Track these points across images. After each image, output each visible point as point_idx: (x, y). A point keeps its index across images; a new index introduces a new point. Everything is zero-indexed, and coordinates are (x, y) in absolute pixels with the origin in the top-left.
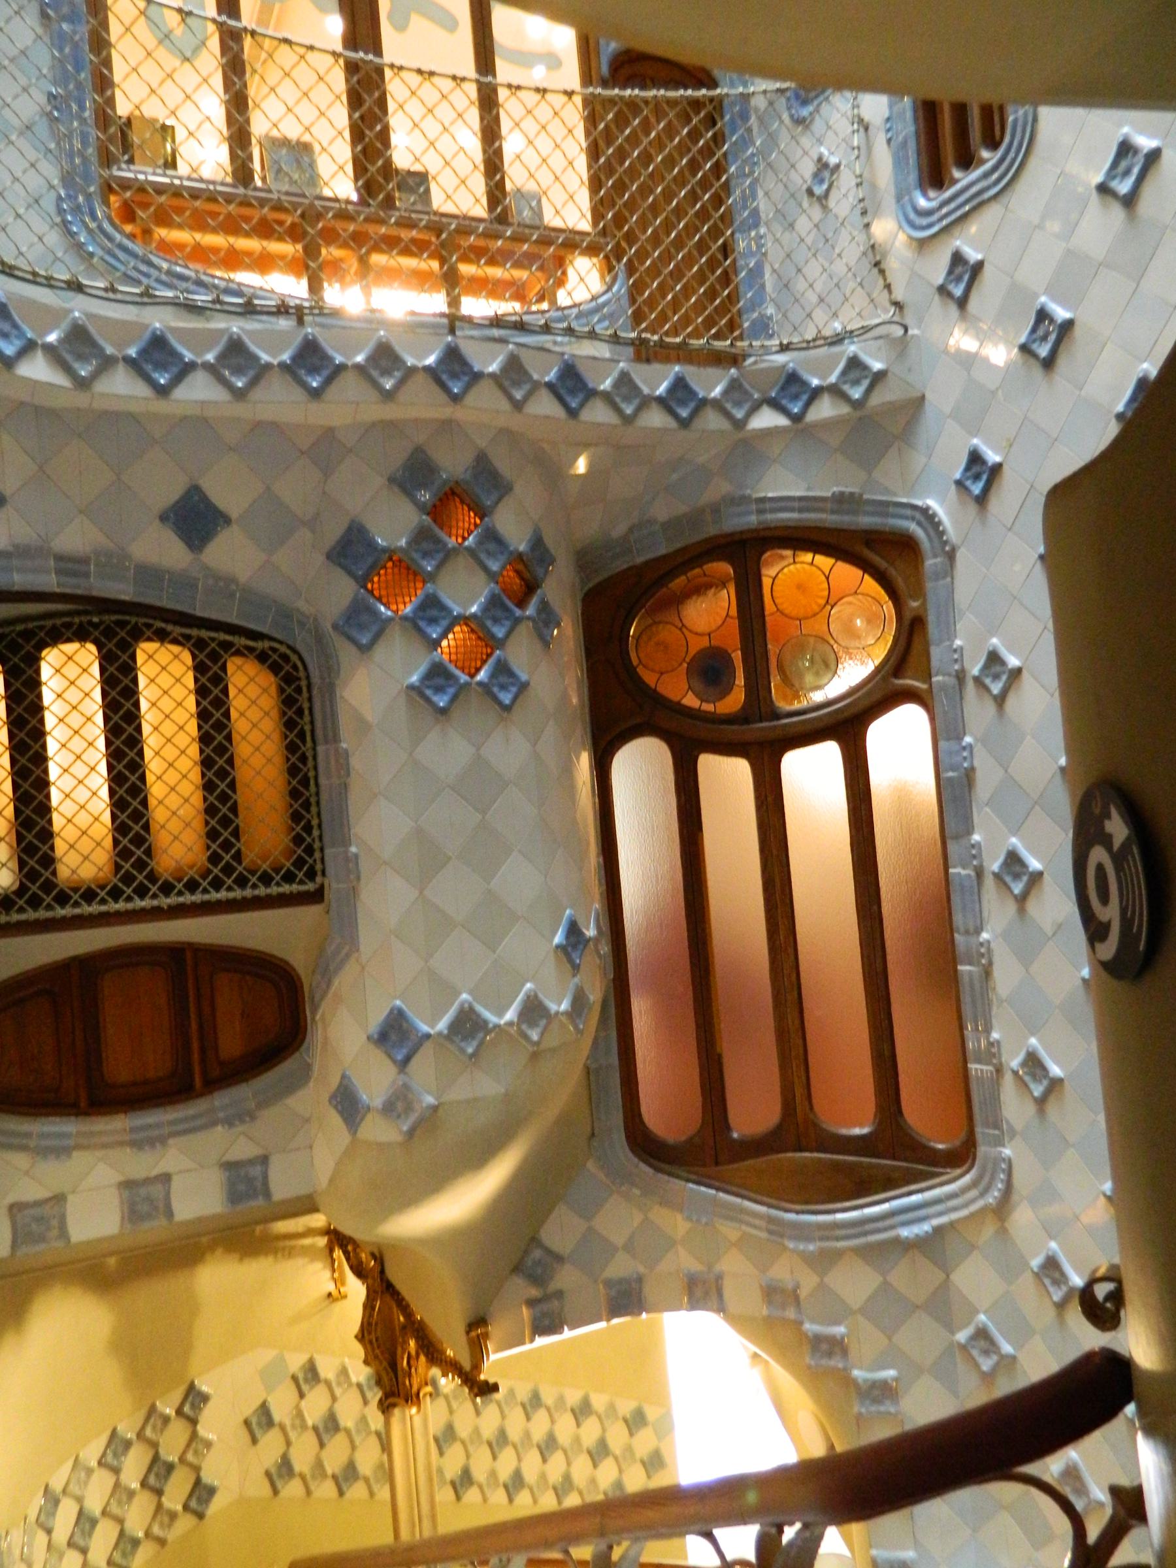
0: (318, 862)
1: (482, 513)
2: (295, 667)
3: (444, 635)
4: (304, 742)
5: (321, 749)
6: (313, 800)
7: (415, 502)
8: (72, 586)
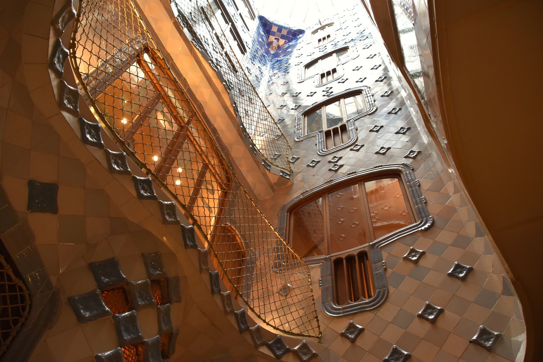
2: (24, 308)
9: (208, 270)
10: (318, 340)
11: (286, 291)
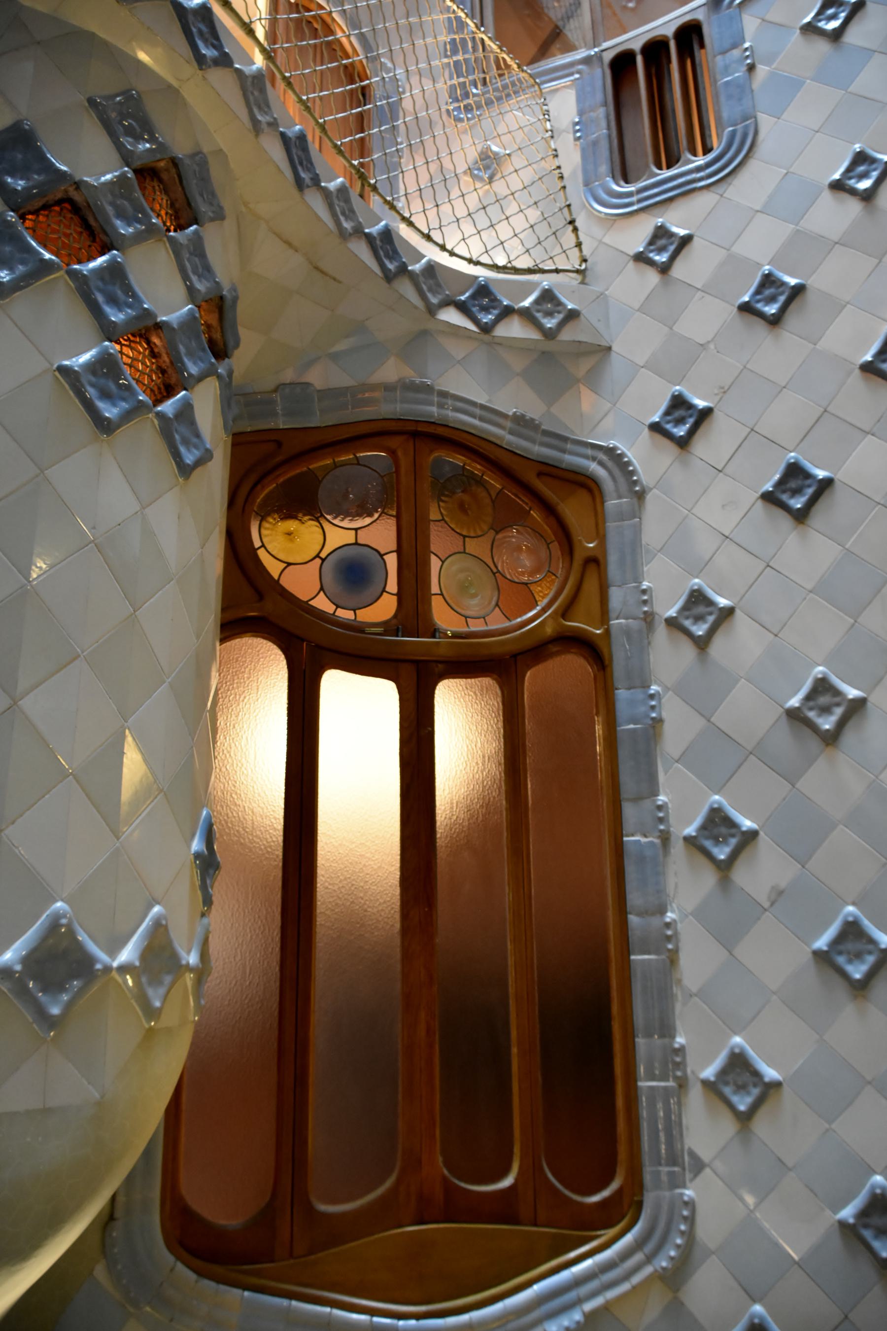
9: (274, 124)
10: (579, 278)
11: (488, 165)
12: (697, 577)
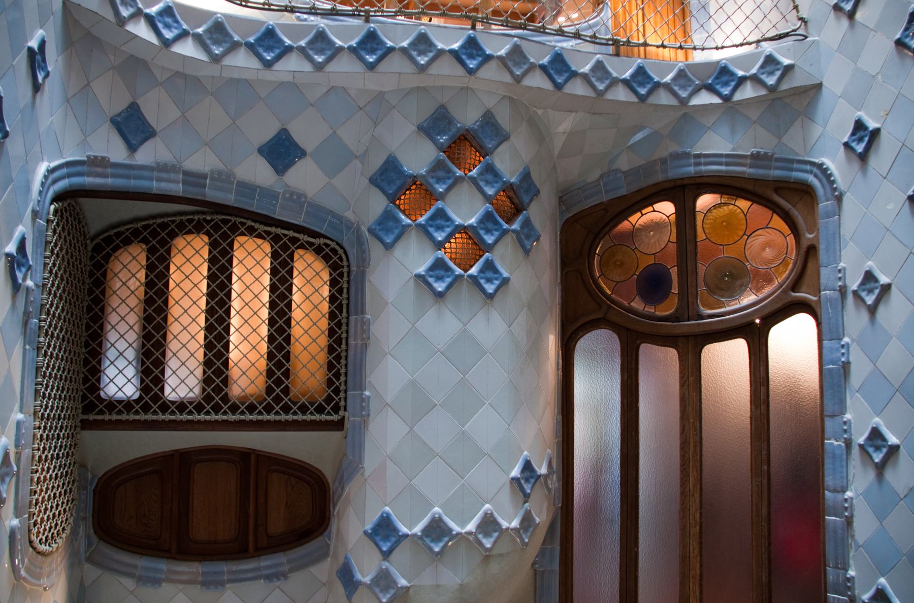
0: (343, 400)
1: (484, 153)
2: (341, 259)
3: (447, 240)
4: (341, 312)
5: (352, 318)
6: (343, 354)
7: (435, 142)
8: (193, 193)
12: (870, 260)
